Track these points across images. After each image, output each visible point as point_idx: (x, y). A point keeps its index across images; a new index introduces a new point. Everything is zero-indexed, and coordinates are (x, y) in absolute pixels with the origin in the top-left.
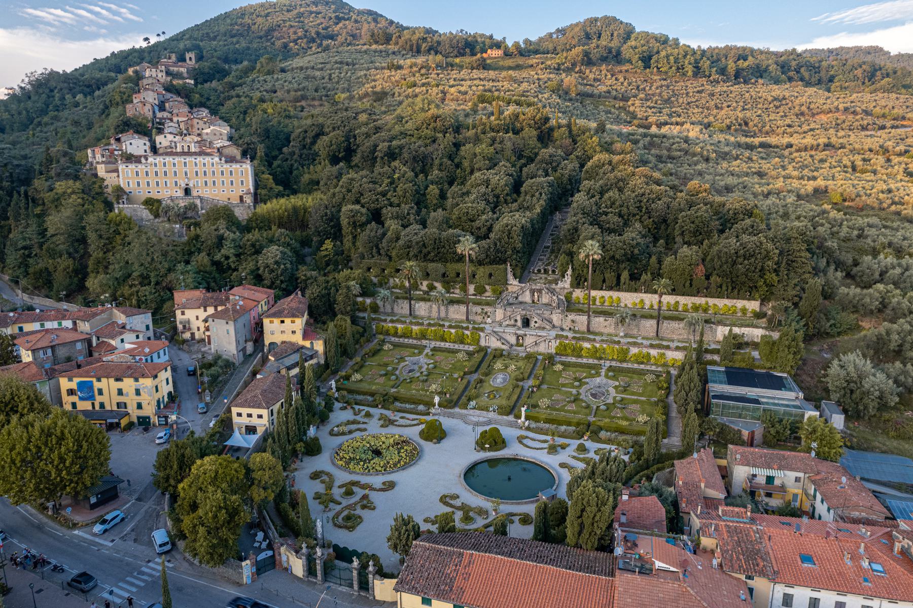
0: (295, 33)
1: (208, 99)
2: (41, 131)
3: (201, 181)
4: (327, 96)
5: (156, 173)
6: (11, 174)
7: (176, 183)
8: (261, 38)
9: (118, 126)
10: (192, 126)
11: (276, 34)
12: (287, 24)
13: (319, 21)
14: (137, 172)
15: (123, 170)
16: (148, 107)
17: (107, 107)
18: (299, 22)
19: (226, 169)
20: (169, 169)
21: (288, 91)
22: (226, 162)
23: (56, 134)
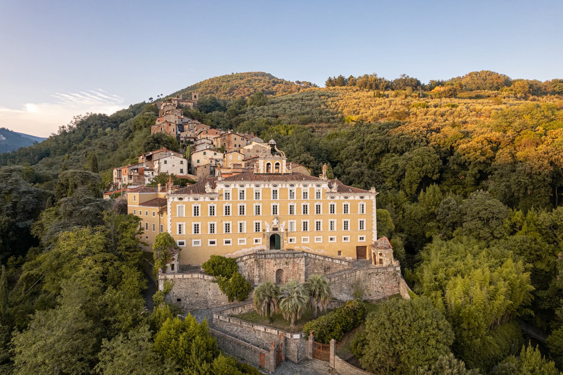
0: (248, 91)
1: (218, 124)
2: (75, 154)
3: (296, 224)
4: (333, 118)
5: (227, 209)
6: (15, 204)
7: (258, 225)
8: (226, 94)
9: (149, 143)
10: (229, 142)
11: (235, 91)
12: (243, 85)
13: (262, 84)
14: (196, 209)
15: (174, 204)
16: (173, 126)
17: (130, 132)
18: (249, 84)
19: (339, 202)
20: (250, 203)
21: (292, 115)
22: (340, 190)
23: (86, 156)
